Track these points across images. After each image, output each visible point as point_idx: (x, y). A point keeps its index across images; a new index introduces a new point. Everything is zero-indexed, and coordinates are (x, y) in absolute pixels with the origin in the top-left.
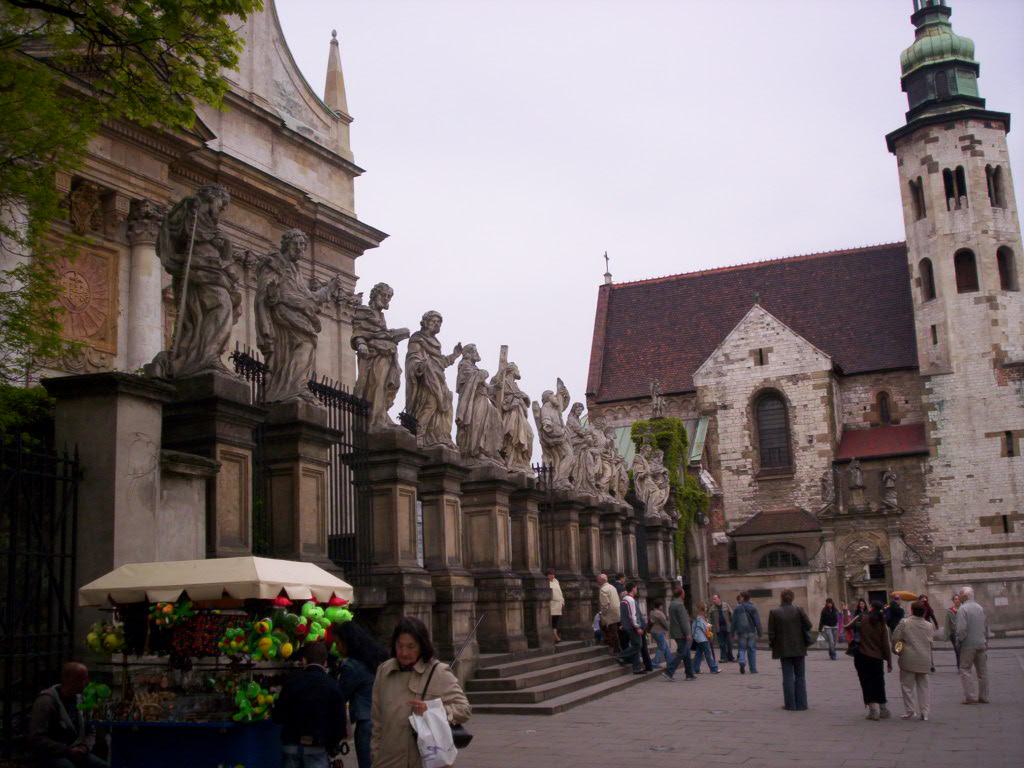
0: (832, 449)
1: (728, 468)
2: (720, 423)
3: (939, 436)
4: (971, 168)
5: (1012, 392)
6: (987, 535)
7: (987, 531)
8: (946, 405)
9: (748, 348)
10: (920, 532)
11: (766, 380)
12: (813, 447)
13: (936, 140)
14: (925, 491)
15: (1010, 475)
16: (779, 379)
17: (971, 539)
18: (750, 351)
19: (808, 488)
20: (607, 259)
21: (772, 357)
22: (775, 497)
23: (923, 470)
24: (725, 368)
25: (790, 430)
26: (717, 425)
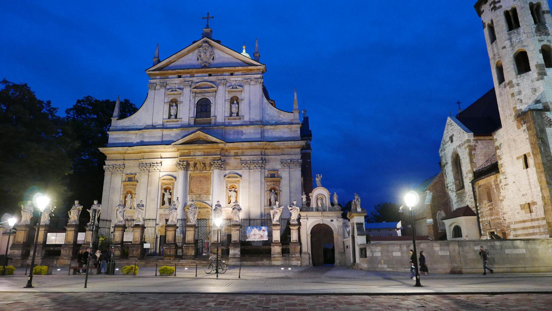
1: (450, 189)
3: (502, 162)
5: (522, 132)
6: (524, 215)
7: (523, 211)
8: (502, 145)
11: (454, 148)
12: (467, 176)
13: (483, 11)
14: (500, 193)
17: (519, 218)
18: (450, 137)
19: (469, 195)
20: (459, 103)
21: (454, 138)
22: (461, 201)
23: (499, 183)
24: (445, 146)
25: (461, 170)
26: (446, 172)
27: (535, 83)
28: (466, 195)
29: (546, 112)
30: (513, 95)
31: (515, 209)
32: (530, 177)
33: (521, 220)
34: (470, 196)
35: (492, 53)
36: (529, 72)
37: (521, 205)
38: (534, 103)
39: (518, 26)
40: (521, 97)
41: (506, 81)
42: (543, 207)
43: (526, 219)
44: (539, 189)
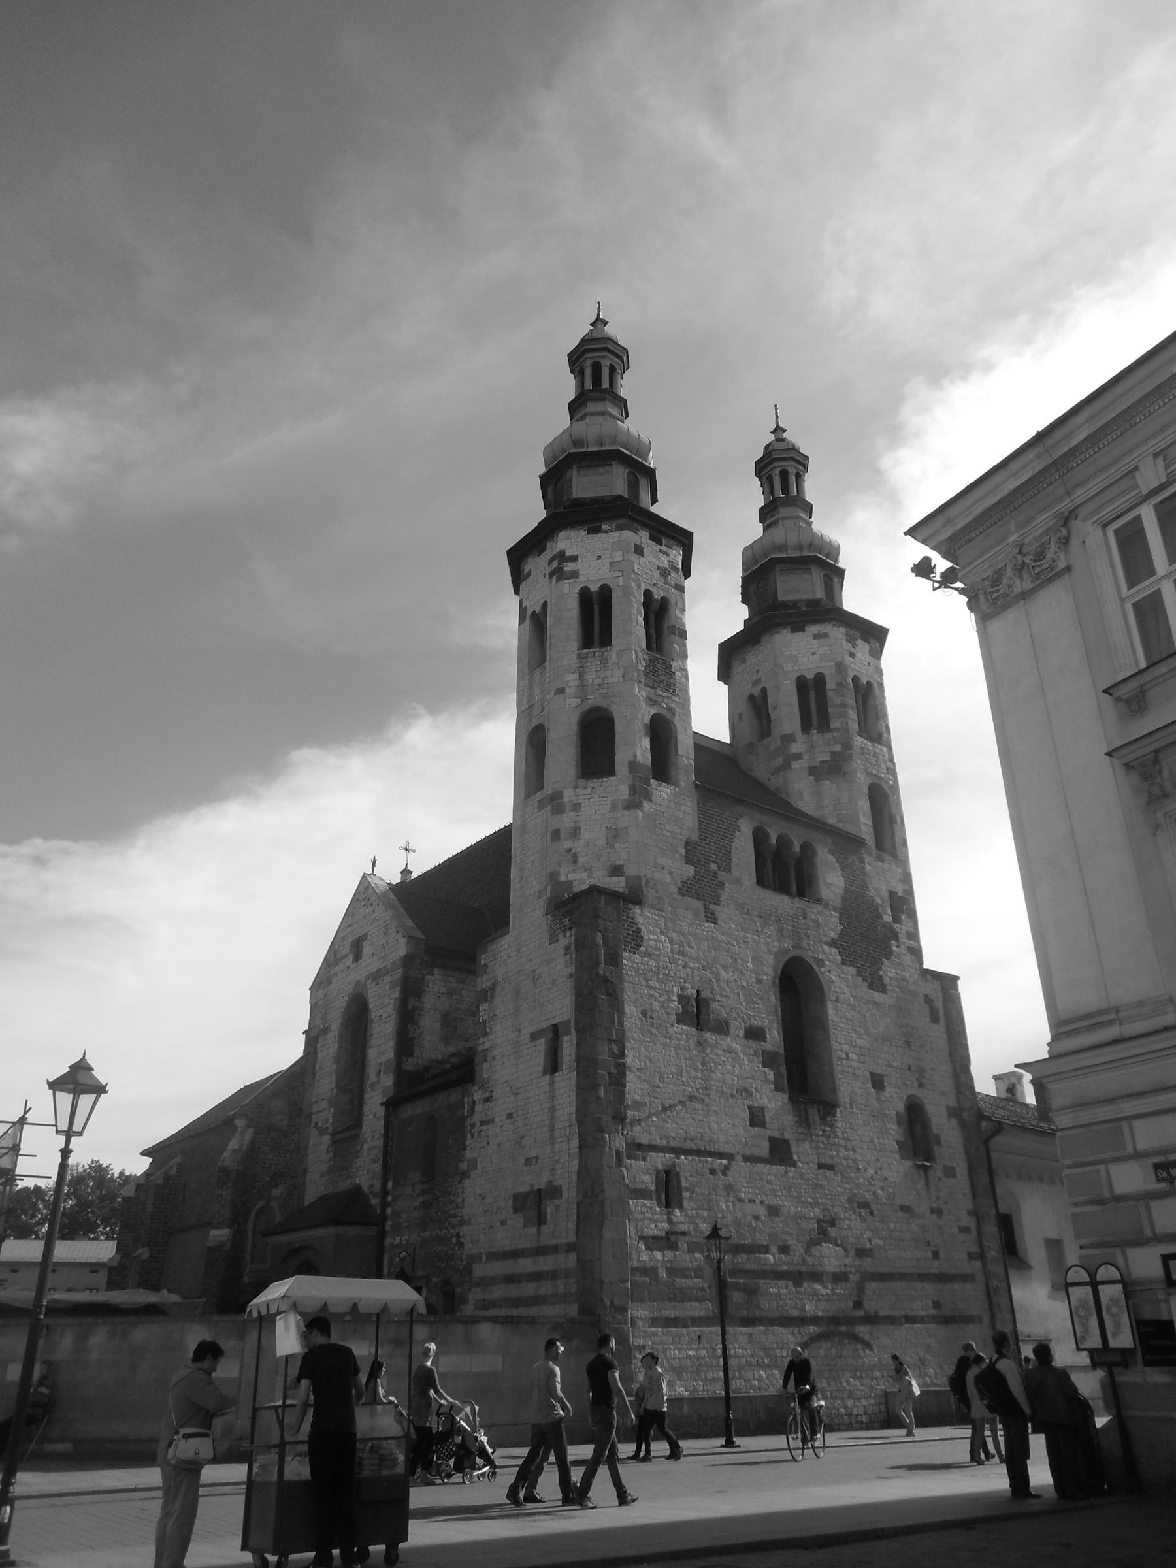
0: (394, 1084)
1: (316, 1124)
2: (319, 1055)
3: (487, 1045)
4: (554, 601)
5: (562, 952)
8: (498, 990)
9: (351, 940)
10: (453, 1227)
11: (358, 982)
12: (379, 1081)
13: (529, 574)
14: (465, 1149)
15: (549, 1108)
16: (367, 978)
17: (503, 1239)
19: (370, 1150)
20: (407, 850)
21: (367, 949)
23: (466, 1114)
26: (315, 1060)
27: (620, 813)
28: (362, 1147)
29: (631, 906)
30: (556, 835)
31: (498, 1208)
32: (556, 1103)
33: (508, 1248)
34: (372, 1152)
35: (525, 701)
36: (610, 779)
37: (516, 1197)
38: (606, 873)
39: (606, 641)
40: (578, 846)
41: (548, 790)
42: (575, 1206)
43: (523, 1246)
44: (575, 1143)
